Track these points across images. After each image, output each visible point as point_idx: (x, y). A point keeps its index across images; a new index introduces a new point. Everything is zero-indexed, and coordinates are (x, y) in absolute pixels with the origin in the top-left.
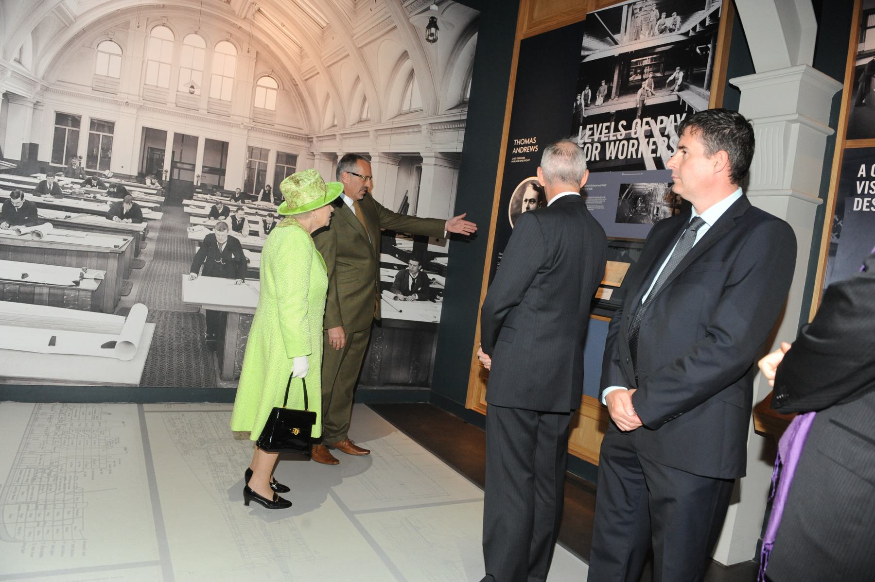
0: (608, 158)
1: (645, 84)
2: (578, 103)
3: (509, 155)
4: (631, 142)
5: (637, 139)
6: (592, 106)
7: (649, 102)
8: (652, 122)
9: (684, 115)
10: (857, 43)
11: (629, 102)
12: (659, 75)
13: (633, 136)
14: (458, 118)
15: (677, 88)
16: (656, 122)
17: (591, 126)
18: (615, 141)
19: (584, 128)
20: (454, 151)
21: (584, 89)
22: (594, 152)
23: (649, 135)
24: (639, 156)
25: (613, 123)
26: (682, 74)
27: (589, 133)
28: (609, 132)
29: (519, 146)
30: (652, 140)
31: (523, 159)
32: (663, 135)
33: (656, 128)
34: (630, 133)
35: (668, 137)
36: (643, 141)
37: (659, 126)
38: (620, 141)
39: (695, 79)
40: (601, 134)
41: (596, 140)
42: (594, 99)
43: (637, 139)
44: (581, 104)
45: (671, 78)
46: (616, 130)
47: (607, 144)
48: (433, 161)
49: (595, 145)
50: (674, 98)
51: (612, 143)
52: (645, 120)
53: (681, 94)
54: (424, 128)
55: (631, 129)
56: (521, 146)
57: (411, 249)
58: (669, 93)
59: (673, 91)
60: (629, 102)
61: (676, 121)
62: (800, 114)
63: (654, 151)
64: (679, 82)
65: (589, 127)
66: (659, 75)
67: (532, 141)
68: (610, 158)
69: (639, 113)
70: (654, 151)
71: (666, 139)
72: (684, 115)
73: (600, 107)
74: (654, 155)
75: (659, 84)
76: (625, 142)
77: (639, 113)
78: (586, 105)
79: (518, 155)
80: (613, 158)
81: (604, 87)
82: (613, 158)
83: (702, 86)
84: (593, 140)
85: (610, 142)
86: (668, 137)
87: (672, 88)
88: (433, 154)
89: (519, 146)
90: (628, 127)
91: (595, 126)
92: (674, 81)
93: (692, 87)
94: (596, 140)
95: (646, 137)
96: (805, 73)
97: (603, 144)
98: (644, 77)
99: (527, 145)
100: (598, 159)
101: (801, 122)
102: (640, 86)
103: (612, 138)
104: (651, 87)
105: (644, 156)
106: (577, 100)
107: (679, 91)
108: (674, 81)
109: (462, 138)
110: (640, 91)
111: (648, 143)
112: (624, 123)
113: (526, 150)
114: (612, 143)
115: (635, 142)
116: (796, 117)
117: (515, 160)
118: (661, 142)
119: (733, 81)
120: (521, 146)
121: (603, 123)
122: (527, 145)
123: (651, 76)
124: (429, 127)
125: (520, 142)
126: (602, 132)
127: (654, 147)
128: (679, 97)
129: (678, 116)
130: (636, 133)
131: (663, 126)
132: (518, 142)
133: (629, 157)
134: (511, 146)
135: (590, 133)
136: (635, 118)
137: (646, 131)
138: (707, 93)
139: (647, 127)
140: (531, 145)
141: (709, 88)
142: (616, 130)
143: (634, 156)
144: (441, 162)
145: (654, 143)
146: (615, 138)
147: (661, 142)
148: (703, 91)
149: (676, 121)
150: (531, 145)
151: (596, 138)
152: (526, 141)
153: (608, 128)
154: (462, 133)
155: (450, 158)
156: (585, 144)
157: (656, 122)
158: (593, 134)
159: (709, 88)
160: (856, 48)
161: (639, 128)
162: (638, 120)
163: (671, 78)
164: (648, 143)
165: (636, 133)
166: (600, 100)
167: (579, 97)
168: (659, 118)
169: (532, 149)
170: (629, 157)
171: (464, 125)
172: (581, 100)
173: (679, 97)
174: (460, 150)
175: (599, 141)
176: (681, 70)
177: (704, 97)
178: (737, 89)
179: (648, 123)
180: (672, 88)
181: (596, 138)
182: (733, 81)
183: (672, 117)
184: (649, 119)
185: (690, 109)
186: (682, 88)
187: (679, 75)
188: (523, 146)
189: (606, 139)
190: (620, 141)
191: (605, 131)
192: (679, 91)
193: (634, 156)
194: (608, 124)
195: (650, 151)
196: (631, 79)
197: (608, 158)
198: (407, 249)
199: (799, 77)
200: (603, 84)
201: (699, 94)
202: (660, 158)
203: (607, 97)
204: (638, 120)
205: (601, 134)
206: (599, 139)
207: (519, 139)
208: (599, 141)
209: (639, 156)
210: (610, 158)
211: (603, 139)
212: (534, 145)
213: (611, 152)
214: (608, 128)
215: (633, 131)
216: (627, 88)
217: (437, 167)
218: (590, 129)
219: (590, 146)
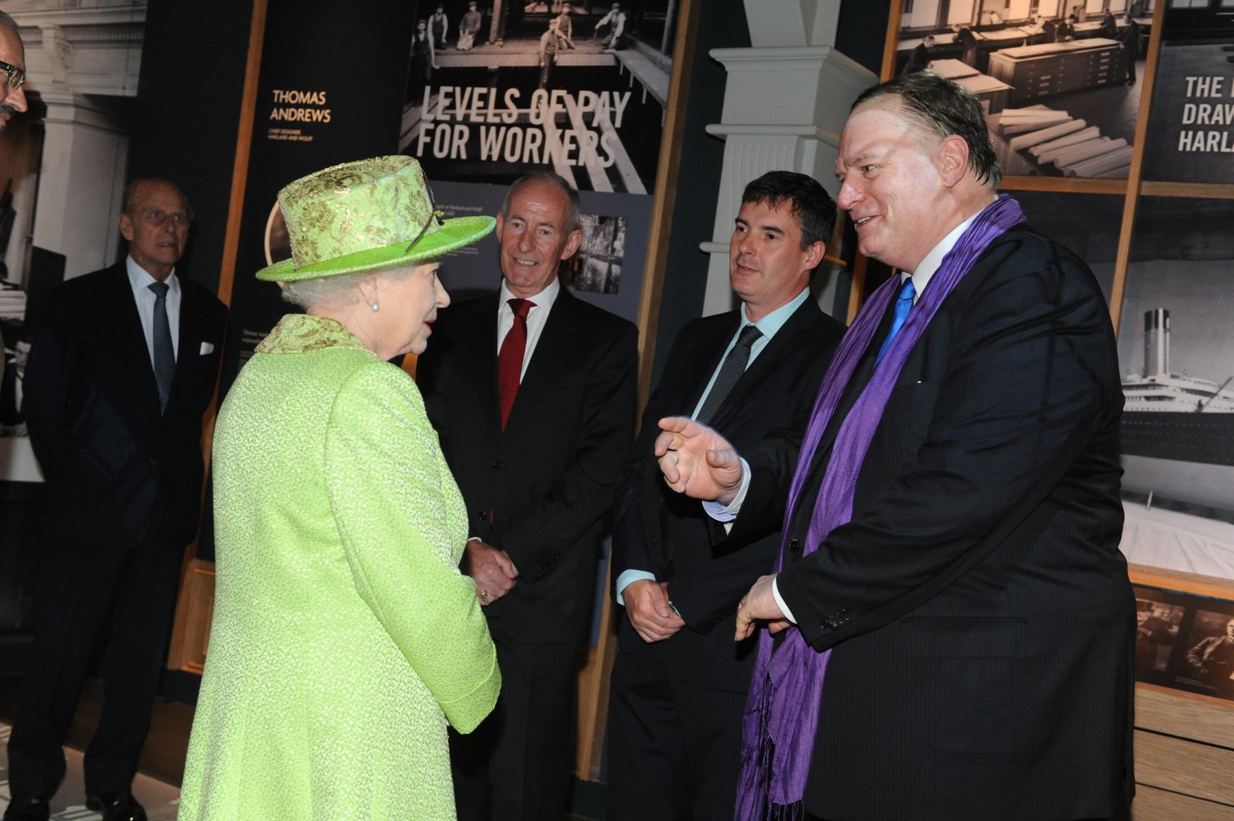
0: (484, 157)
1: (555, 25)
2: (422, 37)
3: (262, 123)
4: (530, 131)
5: (540, 127)
6: (450, 50)
7: (563, 60)
8: (569, 99)
9: (628, 95)
10: (900, 13)
11: (525, 55)
12: (580, 11)
13: (534, 121)
14: (126, 19)
15: (613, 42)
16: (576, 100)
17: (450, 89)
18: (498, 126)
19: (435, 92)
20: (119, 93)
21: (434, 12)
22: (456, 142)
23: (564, 123)
24: (546, 161)
25: (494, 91)
26: (622, 18)
27: (443, 102)
28: (486, 107)
29: (286, 106)
30: (568, 133)
31: (295, 135)
32: (589, 125)
33: (576, 113)
34: (527, 115)
35: (599, 131)
36: (553, 133)
37: (582, 109)
38: (509, 126)
39: (646, 31)
40: (469, 107)
41: (460, 118)
42: (454, 37)
43: (540, 127)
44: (426, 41)
45: (604, 21)
46: (500, 104)
47: (483, 129)
48: (70, 114)
49: (458, 128)
50: (606, 60)
51: (493, 129)
52: (556, 93)
53: (621, 53)
54: (49, 36)
55: (528, 106)
56: (289, 105)
57: (22, 316)
58: (599, 49)
59: (606, 46)
60: (525, 55)
61: (612, 104)
62: (819, 127)
63: (574, 155)
64: (619, 31)
65: (444, 89)
66: (580, 11)
67: (319, 98)
68: (489, 157)
69: (545, 79)
70: (574, 155)
71: (594, 134)
72: (628, 95)
73: (466, 53)
74: (573, 162)
75: (583, 29)
76: (518, 130)
77: (545, 79)
78: (438, 45)
79: (284, 124)
80: (495, 158)
81: (474, 14)
82: (495, 158)
83: (657, 46)
84: (453, 117)
85: (488, 126)
86: (599, 131)
87: (604, 41)
88: (70, 98)
89: (286, 106)
90: (523, 102)
91: (458, 90)
92: (610, 27)
93: (641, 45)
94: (460, 118)
95: (558, 126)
96: (828, 60)
97: (474, 128)
98: (554, 9)
99: (305, 106)
100: (464, 156)
101: (820, 139)
102: (545, 27)
103: (491, 119)
104: (566, 33)
105: (555, 162)
106: (418, 32)
107: (618, 48)
108: (610, 27)
109: (136, 65)
110: (546, 37)
111: (562, 137)
112: (516, 92)
113: (301, 115)
114: (493, 129)
115: (538, 132)
116: (812, 130)
117: (275, 134)
118: (587, 142)
119: (715, 54)
120: (289, 105)
121: (473, 86)
122: (305, 106)
123: (566, 10)
124: (61, 34)
125: (287, 97)
126: (472, 104)
127: (573, 147)
128: (617, 59)
129: (616, 95)
130: (538, 116)
131: (588, 109)
132: (280, 95)
133: (526, 160)
134: (265, 103)
135: (447, 102)
136: (537, 88)
137: (558, 115)
138: (667, 61)
139: (559, 108)
140: (314, 106)
141: (670, 52)
142: (500, 104)
143: (536, 160)
144: (86, 117)
145: (573, 140)
146: (497, 120)
147: (587, 142)
148: (659, 55)
149: (612, 104)
150: (314, 106)
151: (460, 113)
152: (301, 97)
153: (484, 98)
154: (136, 54)
155: (104, 110)
156: (437, 123)
157: (576, 100)
158: (452, 106)
159: (670, 52)
160: (899, 21)
161: (544, 107)
162: (541, 92)
163: (604, 21)
164: (562, 137)
165: (538, 116)
166: (466, 41)
167: (422, 26)
168: (583, 94)
169: (318, 115)
170: (526, 160)
171: (140, 36)
172: (426, 32)
173: (617, 59)
174: (131, 92)
175: (466, 120)
176: (621, 9)
177: (662, 67)
178: (720, 66)
179: (560, 100)
180: (604, 41)
181: (460, 113)
182: (715, 54)
183: (605, 95)
184: (563, 93)
185: (638, 87)
186: (623, 44)
187: (617, 19)
188: (298, 106)
189: (481, 119)
190: (509, 126)
191: (477, 103)
192: (619, 47)
193: (536, 160)
194: (484, 90)
195: (566, 154)
196: (528, 9)
197: (484, 157)
198: (11, 316)
199: (818, 66)
200: (473, 8)
201: (654, 61)
202: (584, 168)
203: (481, 38)
204: (541, 92)
205: (469, 107)
206: (467, 117)
207: (285, 90)
208: (466, 120)
209: (546, 161)
210: (489, 157)
211: (474, 118)
212: (321, 108)
213: (490, 147)
214: (484, 98)
215: (532, 111)
216: (522, 27)
217: (80, 129)
218: (447, 95)
219: (447, 127)
